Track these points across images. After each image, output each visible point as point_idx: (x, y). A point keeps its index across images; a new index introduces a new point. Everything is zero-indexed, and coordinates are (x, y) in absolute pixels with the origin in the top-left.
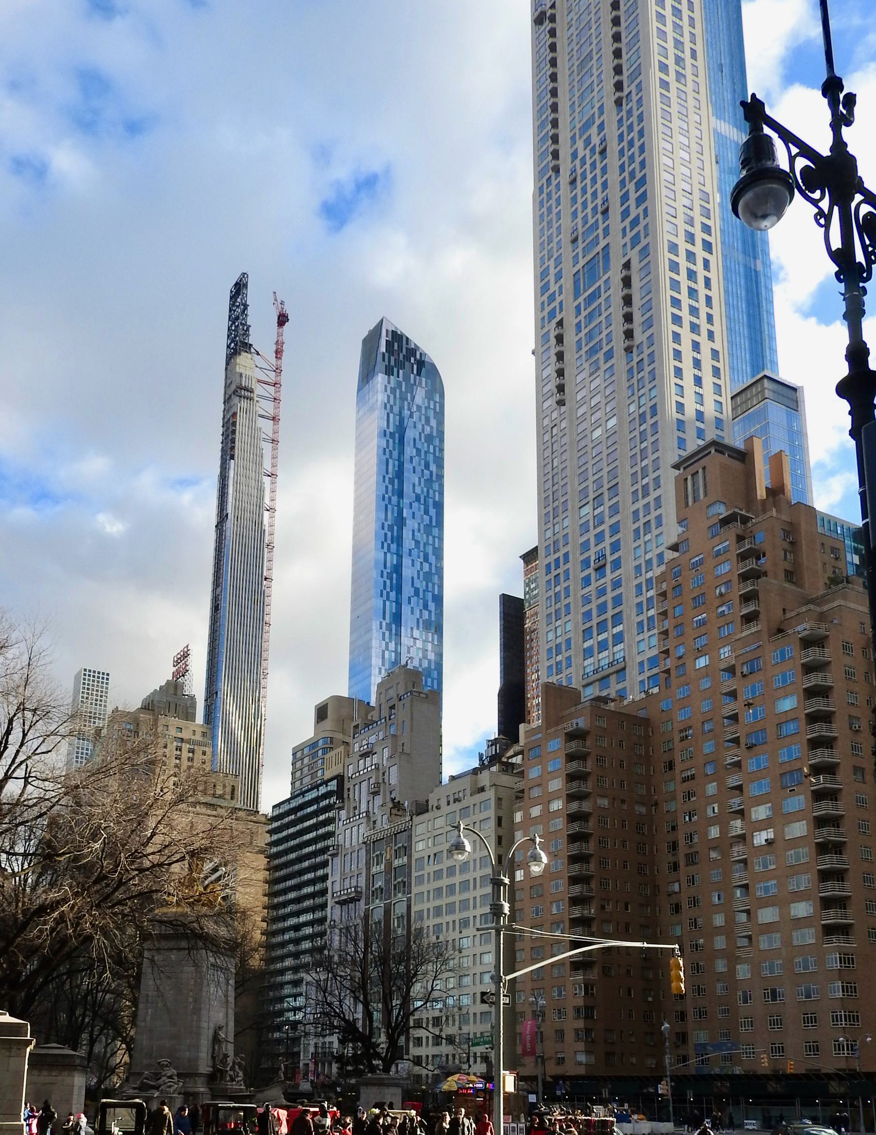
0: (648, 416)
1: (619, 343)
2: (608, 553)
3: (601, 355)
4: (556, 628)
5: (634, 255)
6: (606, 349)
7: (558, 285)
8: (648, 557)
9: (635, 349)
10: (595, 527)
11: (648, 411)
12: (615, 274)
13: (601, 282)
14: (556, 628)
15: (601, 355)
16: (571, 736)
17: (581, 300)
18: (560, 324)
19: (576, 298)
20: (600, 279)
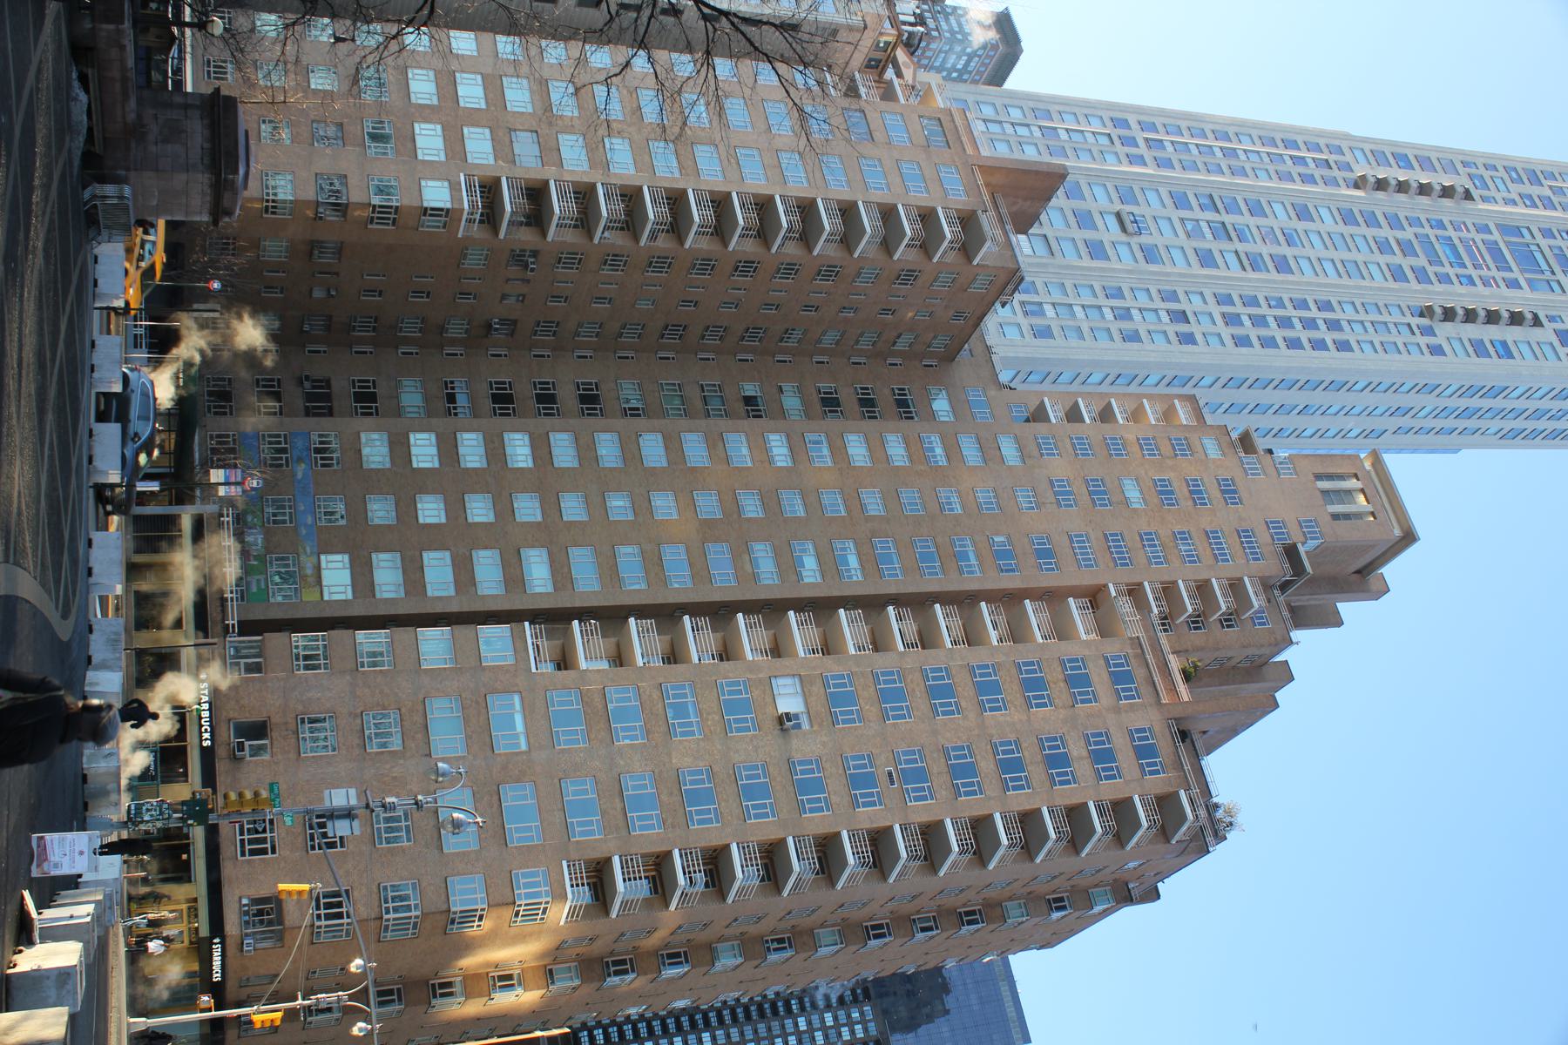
0: (1337, 336)
1: (1440, 295)
2: (1144, 239)
3: (1422, 261)
4: (1028, 125)
5: (1547, 334)
6: (1430, 270)
7: (1517, 199)
8: (1135, 312)
9: (1425, 321)
10: (1182, 220)
11: (1345, 337)
12: (1522, 299)
13: (1516, 274)
14: (1028, 125)
15: (1422, 261)
16: (967, 221)
17: (1496, 236)
18: (1468, 196)
19: (1500, 227)
20: (1522, 271)
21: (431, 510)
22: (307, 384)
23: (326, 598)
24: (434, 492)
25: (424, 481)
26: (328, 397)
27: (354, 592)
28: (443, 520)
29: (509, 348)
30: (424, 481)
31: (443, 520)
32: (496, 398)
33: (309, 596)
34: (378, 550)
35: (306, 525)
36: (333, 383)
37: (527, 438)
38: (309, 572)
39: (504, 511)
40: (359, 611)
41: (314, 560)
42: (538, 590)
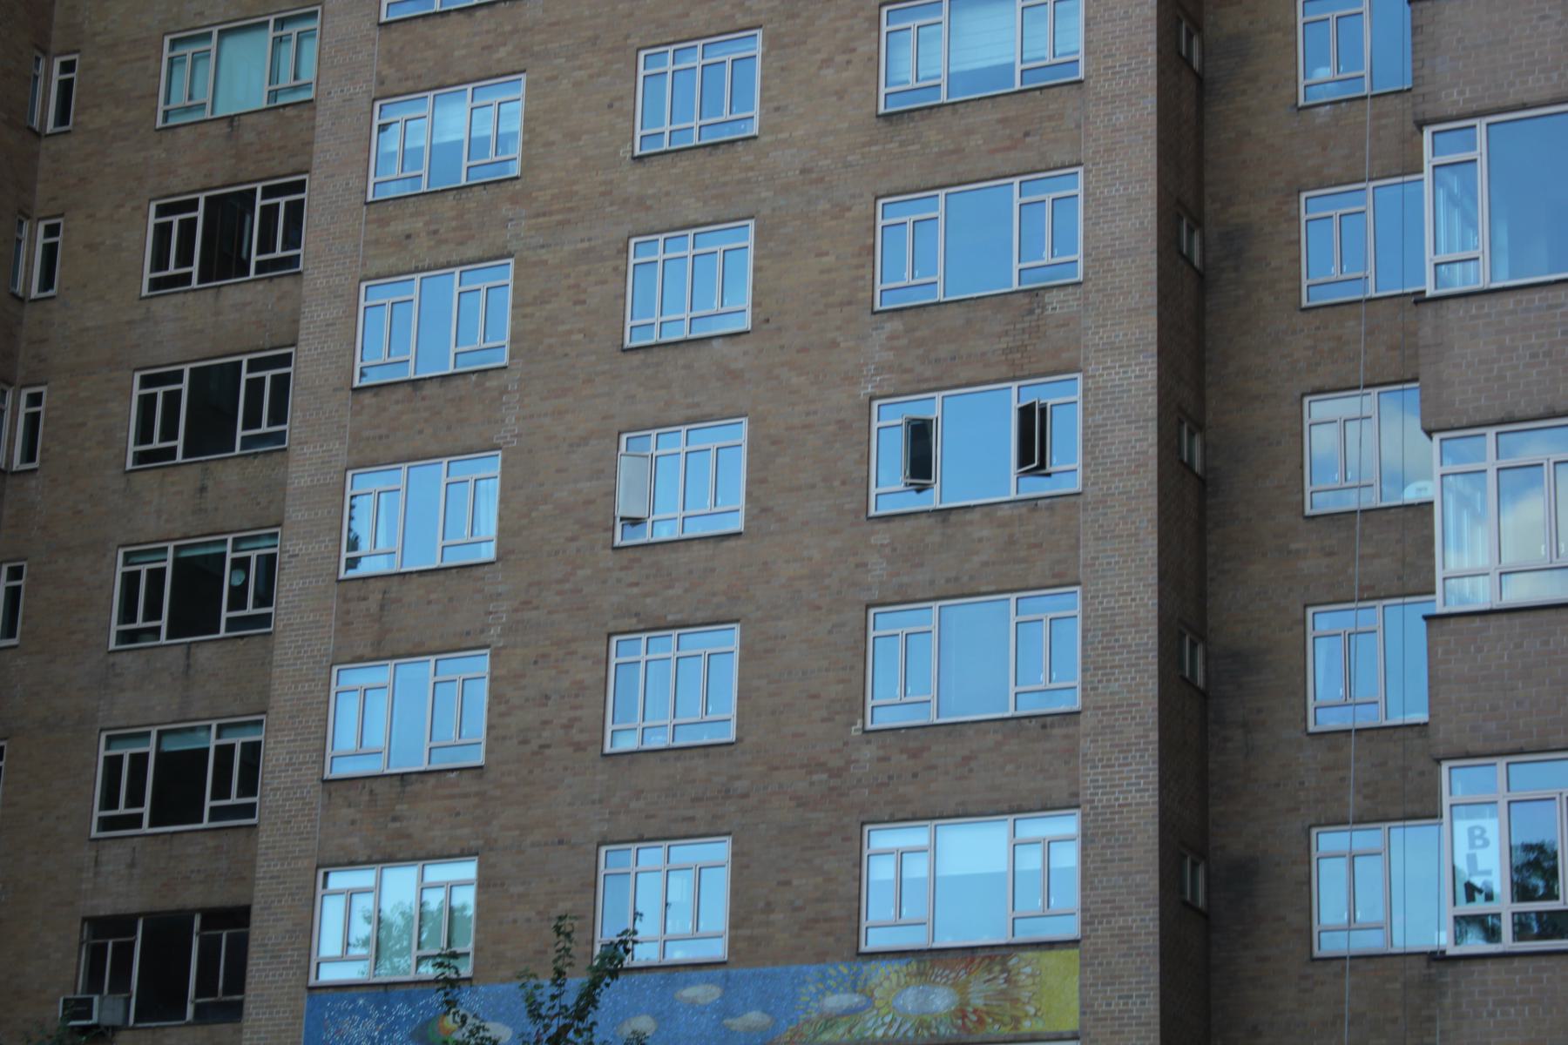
21: (689, 483)
22: (104, 1010)
23: (1070, 928)
24: (606, 473)
25: (562, 522)
26: (167, 931)
27: (1047, 806)
28: (739, 432)
29: (24, 214)
30: (562, 522)
31: (739, 432)
32: (225, 262)
33: (1056, 997)
34: (856, 704)
35: (725, 1010)
36: (106, 906)
37: (397, 112)
38: (941, 1000)
39: (709, 179)
40: (1135, 785)
41: (882, 973)
42: (1074, 40)
